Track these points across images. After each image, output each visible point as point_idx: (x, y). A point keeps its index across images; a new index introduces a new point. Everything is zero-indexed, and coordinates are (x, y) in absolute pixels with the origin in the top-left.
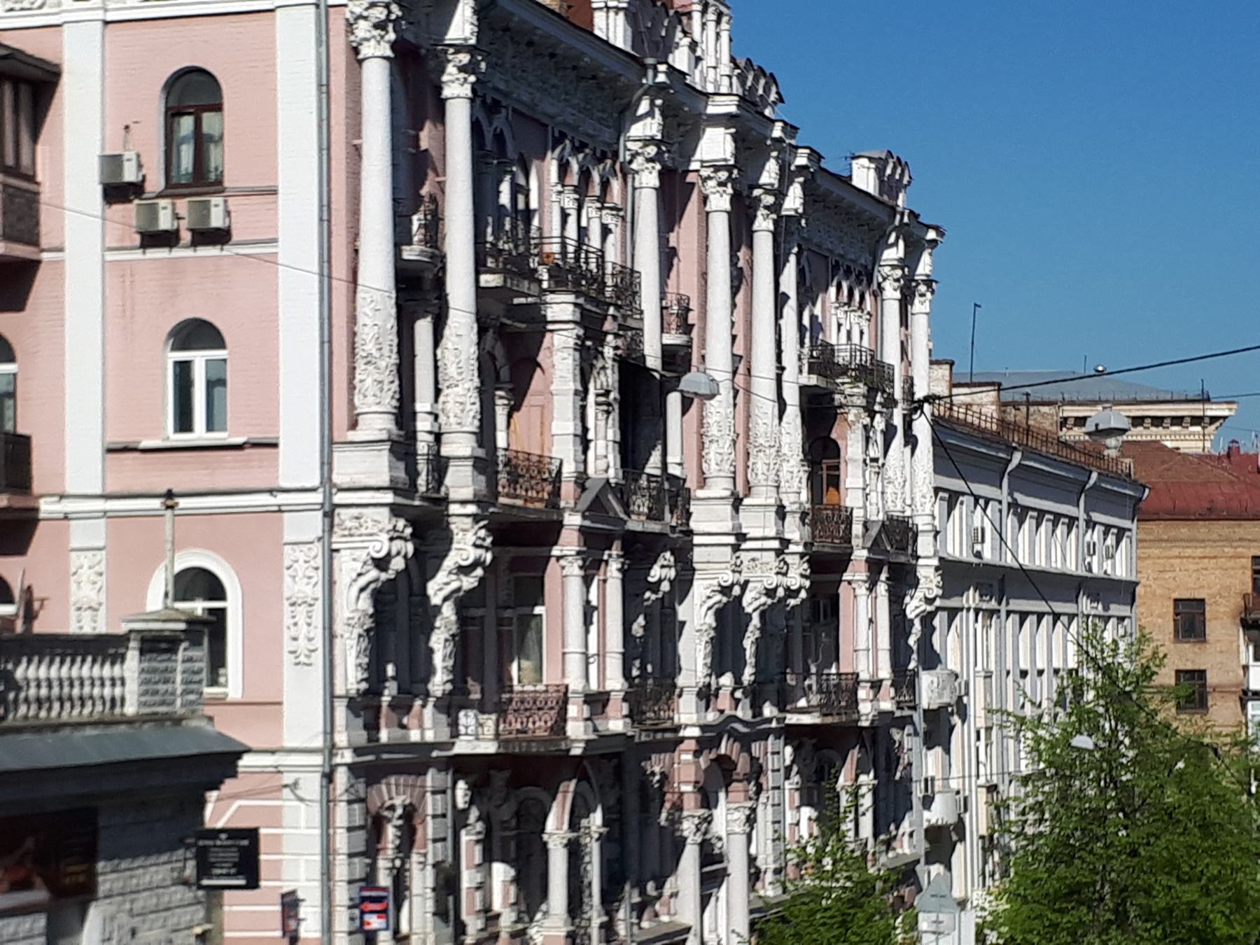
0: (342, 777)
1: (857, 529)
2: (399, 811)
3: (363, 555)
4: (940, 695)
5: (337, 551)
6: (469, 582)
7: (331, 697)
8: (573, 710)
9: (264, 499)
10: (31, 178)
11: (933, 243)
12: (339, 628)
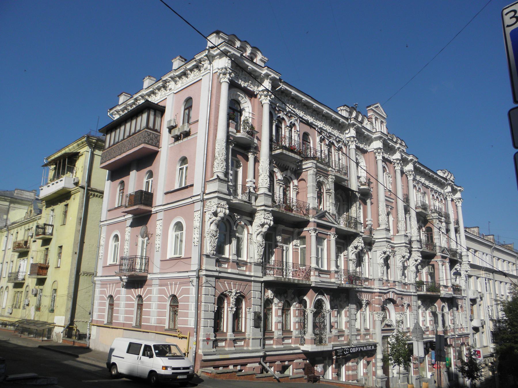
0: (204, 279)
1: (437, 248)
2: (234, 294)
3: (210, 212)
4: (474, 295)
5: (205, 212)
6: (265, 229)
7: (201, 255)
8: (312, 273)
9: (190, 200)
10: (160, 132)
11: (460, 190)
12: (206, 235)
